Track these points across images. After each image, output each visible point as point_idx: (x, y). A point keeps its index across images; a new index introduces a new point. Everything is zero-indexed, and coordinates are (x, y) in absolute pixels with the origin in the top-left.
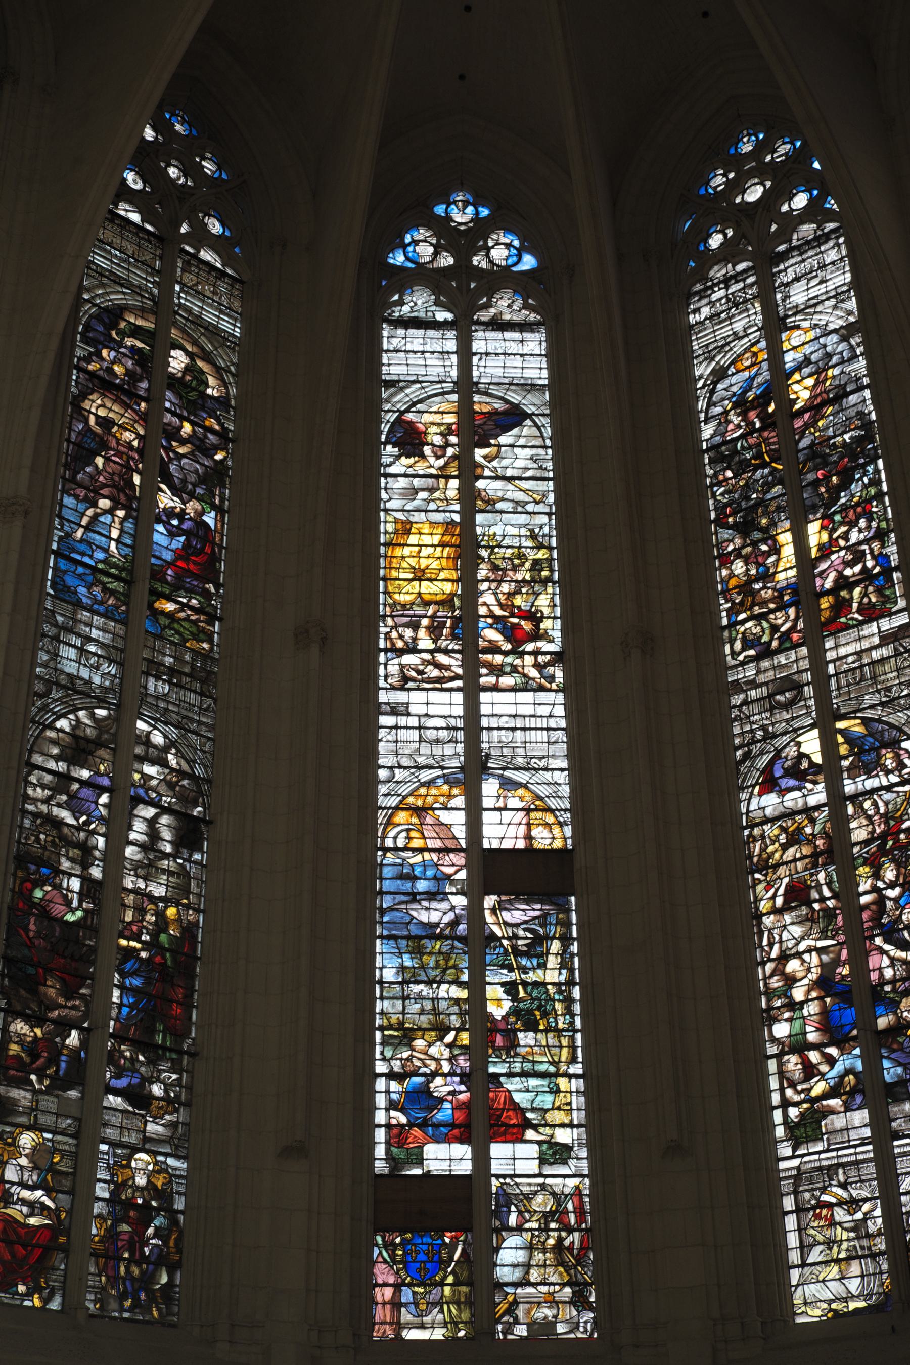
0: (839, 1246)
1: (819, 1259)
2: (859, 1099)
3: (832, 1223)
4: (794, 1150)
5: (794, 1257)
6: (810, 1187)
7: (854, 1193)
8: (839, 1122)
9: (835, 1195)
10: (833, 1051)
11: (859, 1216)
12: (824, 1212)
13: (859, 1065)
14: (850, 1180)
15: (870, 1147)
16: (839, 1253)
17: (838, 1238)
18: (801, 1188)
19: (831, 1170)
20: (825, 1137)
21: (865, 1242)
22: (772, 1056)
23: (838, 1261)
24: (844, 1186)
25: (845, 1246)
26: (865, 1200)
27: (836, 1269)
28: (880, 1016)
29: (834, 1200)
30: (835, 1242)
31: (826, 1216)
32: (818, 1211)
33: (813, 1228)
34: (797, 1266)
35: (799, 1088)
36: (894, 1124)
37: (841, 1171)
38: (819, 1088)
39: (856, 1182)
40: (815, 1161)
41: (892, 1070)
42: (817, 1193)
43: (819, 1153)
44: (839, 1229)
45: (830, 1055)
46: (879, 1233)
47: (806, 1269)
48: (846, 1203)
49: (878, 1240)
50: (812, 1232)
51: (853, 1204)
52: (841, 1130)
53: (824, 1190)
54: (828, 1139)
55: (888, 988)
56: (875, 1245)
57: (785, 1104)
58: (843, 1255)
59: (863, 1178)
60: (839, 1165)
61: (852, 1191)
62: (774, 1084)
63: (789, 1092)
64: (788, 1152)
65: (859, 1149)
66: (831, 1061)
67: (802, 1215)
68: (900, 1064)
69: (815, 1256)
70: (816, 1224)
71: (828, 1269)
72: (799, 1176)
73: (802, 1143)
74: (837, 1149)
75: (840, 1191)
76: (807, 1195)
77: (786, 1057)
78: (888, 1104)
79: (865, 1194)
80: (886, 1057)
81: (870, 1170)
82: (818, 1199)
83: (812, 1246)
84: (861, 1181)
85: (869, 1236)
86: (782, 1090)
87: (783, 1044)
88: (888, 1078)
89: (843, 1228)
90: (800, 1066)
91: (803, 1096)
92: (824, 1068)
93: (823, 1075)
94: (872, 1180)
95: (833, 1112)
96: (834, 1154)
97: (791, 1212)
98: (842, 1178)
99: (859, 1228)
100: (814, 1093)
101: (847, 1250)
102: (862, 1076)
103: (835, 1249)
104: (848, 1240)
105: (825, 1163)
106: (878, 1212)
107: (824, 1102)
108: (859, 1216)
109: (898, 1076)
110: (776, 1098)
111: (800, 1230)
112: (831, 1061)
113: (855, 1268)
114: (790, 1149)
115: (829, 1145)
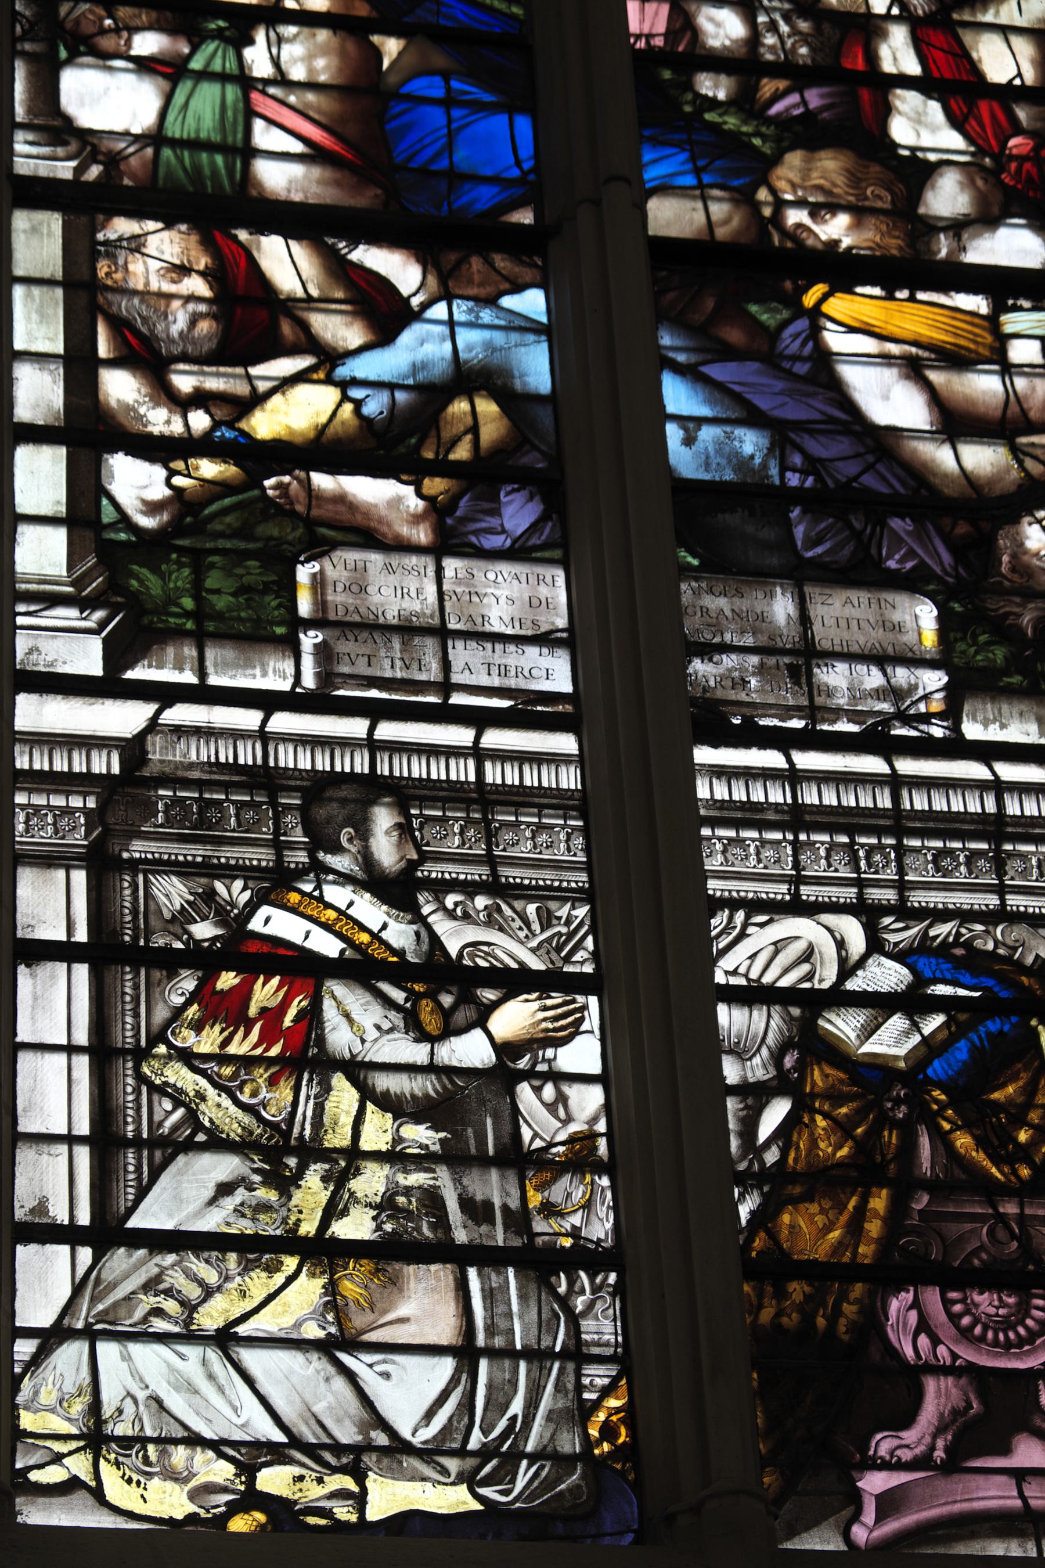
0: (338, 1180)
1: (212, 1222)
2: (518, 514)
3: (307, 1057)
4: (118, 654)
5: (52, 1182)
6: (197, 852)
7: (454, 938)
8: (400, 589)
9: (341, 924)
10: (400, 270)
11: (471, 1050)
12: (265, 993)
13: (535, 367)
14: (434, 870)
15: (566, 743)
16: (332, 1211)
17: (339, 1138)
18: (138, 849)
19: (332, 803)
20: (309, 640)
21: (495, 1188)
22: (39, 194)
23: (323, 1252)
24: (398, 890)
25: (371, 1182)
26: (515, 982)
27: (308, 1291)
28: (664, 189)
29: (328, 946)
30: (312, 1151)
31: (272, 1016)
32: (227, 980)
33: (187, 1057)
34: (69, 1235)
35: (184, 382)
36: (698, 667)
37: (384, 819)
38: (297, 411)
39: (471, 889)
40: (236, 735)
41: (707, 434)
42: (239, 892)
43: (268, 702)
44: (344, 1096)
45: (383, 285)
46: (580, 1157)
47: (119, 1260)
48: (399, 970)
49: (569, 1189)
50: (180, 1076)
51: (441, 989)
52: (408, 630)
53: (275, 885)
54: (323, 652)
55: (713, 87)
56: (549, 1210)
57: (89, 434)
58: (356, 1226)
59: (510, 874)
60: (374, 787)
61: (441, 926)
62: (37, 324)
63: (120, 387)
64: (87, 658)
65: (495, 738)
66: (385, 314)
67: (127, 982)
68: (753, 418)
69: (183, 1196)
70: (207, 1042)
71: (259, 1284)
72: (131, 784)
73: (178, 634)
74: (376, 712)
75: (369, 911)
76: (172, 892)
77: (123, 227)
78: (685, 572)
79: (514, 950)
80: (679, 370)
81: (556, 848)
82: (235, 923)
83: (166, 1149)
84: (495, 888)
85: (516, 1158)
86: (79, 367)
87: (113, 162)
88: (682, 457)
89: (367, 1094)
90: (195, 285)
91: (200, 421)
92: (340, 330)
93: (328, 361)
94: (563, 895)
95: (366, 533)
96: (356, 727)
97: (64, 952)
98: (386, 850)
99: (466, 1111)
100: (265, 424)
101: (386, 1206)
102: (545, 416)
103: (313, 1190)
104: (395, 1157)
105: (286, 757)
106: (583, 1054)
107: (322, 481)
108: (471, 1050)
109: (743, 464)
110: (37, 393)
111: (103, 1052)
112: (385, 314)
113: (425, 1306)
114: (95, 646)
115: (327, 677)
